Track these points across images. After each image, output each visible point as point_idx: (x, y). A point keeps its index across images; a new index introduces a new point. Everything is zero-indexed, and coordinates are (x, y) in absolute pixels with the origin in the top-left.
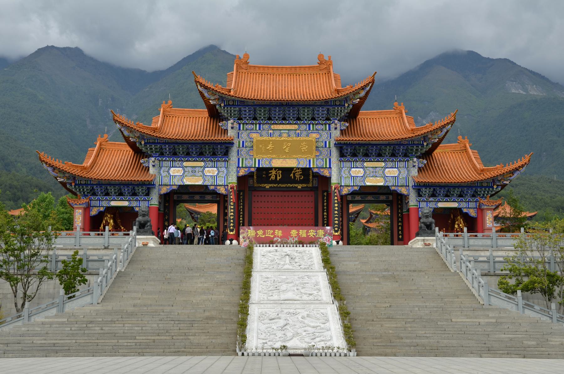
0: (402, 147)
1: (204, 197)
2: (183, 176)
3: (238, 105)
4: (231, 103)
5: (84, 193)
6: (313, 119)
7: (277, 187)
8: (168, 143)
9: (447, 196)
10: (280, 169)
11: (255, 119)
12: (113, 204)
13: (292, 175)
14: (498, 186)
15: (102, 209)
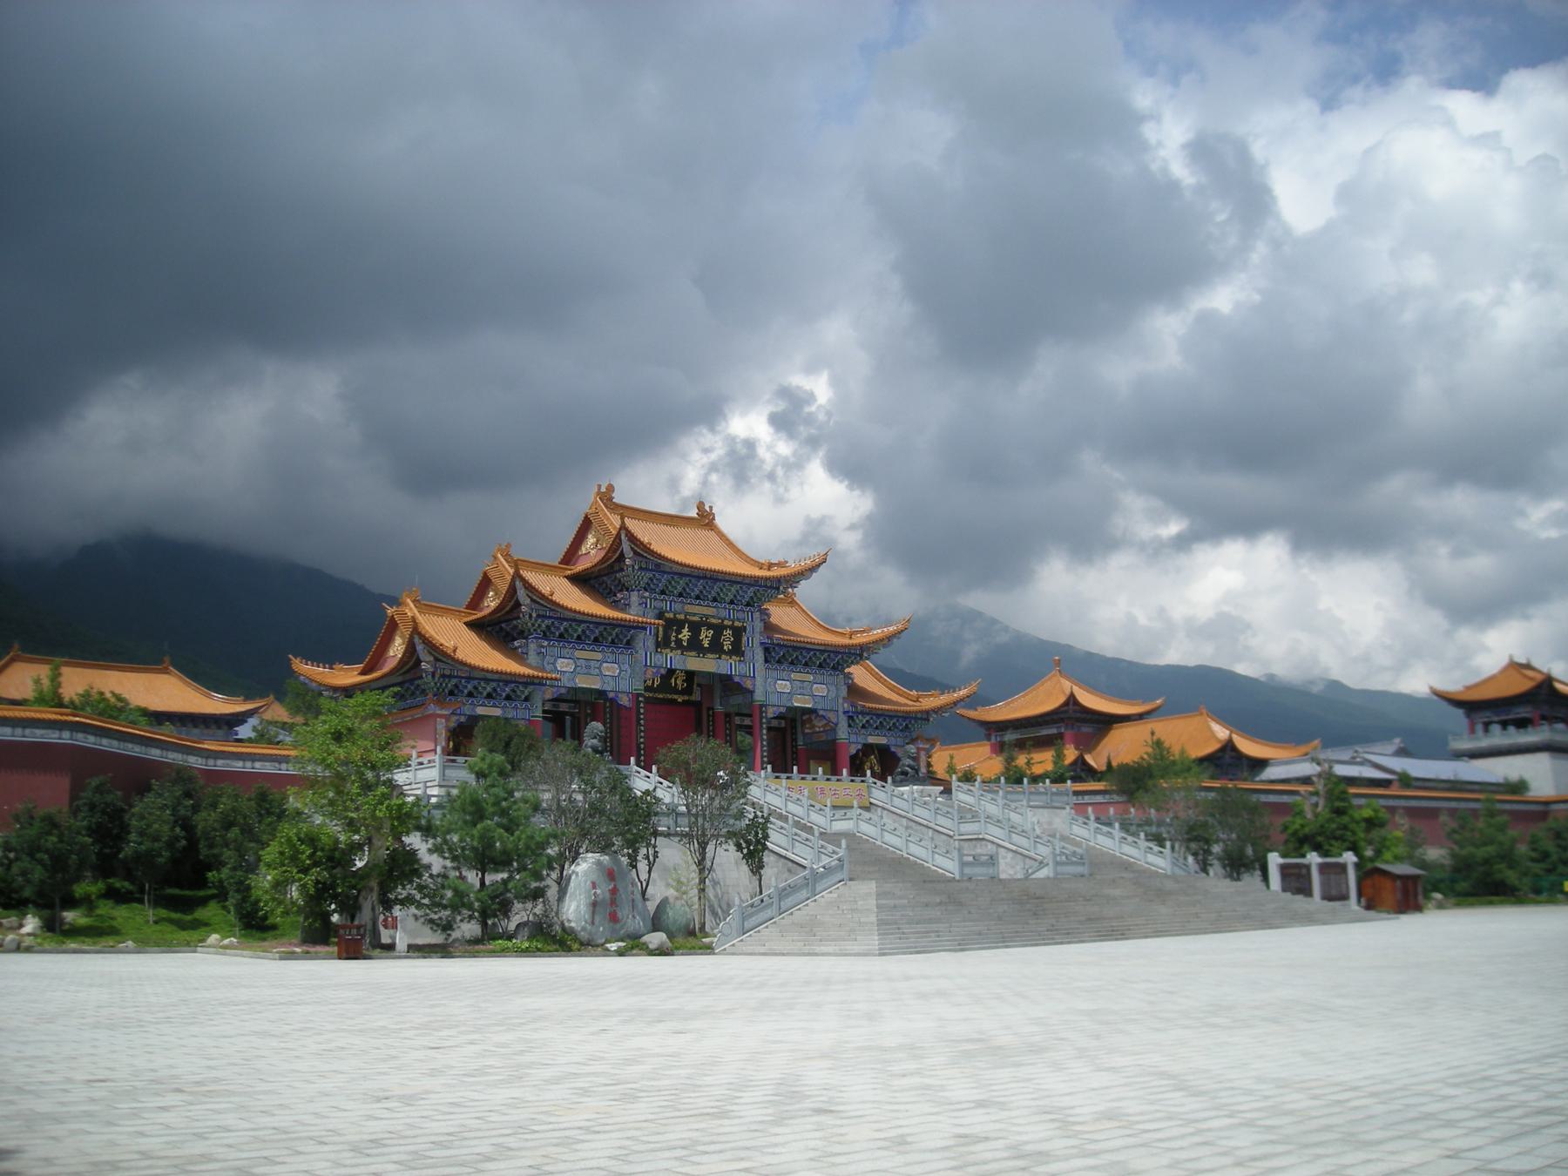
12: (480, 711)
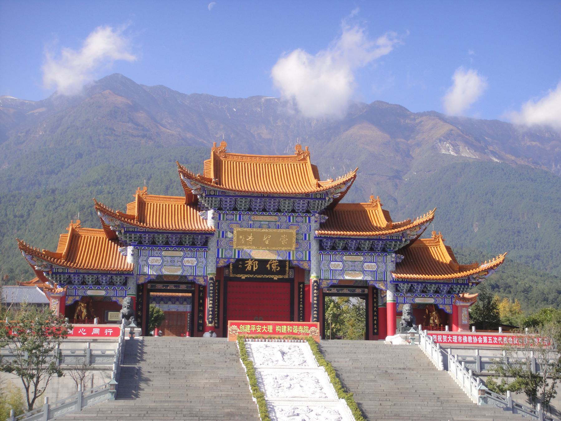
0: (381, 242)
1: (179, 287)
2: (162, 266)
3: (219, 196)
4: (212, 193)
5: (60, 281)
6: (293, 211)
7: (253, 278)
8: (148, 232)
9: (423, 292)
10: (256, 260)
11: (235, 209)
12: (90, 293)
13: (268, 266)
14: (473, 283)
15: (78, 298)
